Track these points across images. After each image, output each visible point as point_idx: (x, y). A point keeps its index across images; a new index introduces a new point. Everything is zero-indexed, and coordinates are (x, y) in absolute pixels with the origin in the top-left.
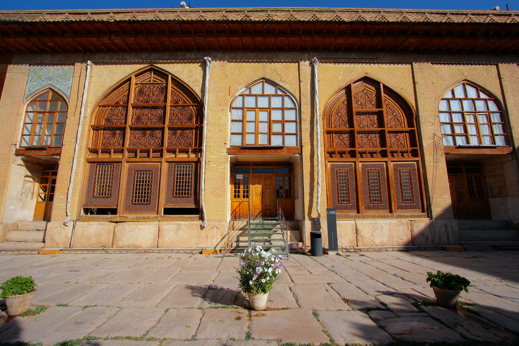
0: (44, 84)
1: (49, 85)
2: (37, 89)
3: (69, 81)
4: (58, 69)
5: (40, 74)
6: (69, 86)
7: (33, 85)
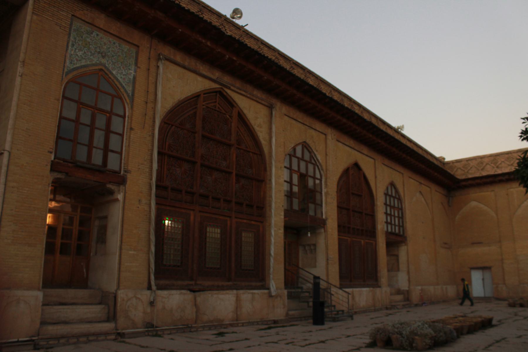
0: (95, 60)
1: (101, 64)
2: (83, 64)
3: (130, 69)
4: (114, 43)
5: (88, 40)
6: (129, 78)
7: (77, 55)
